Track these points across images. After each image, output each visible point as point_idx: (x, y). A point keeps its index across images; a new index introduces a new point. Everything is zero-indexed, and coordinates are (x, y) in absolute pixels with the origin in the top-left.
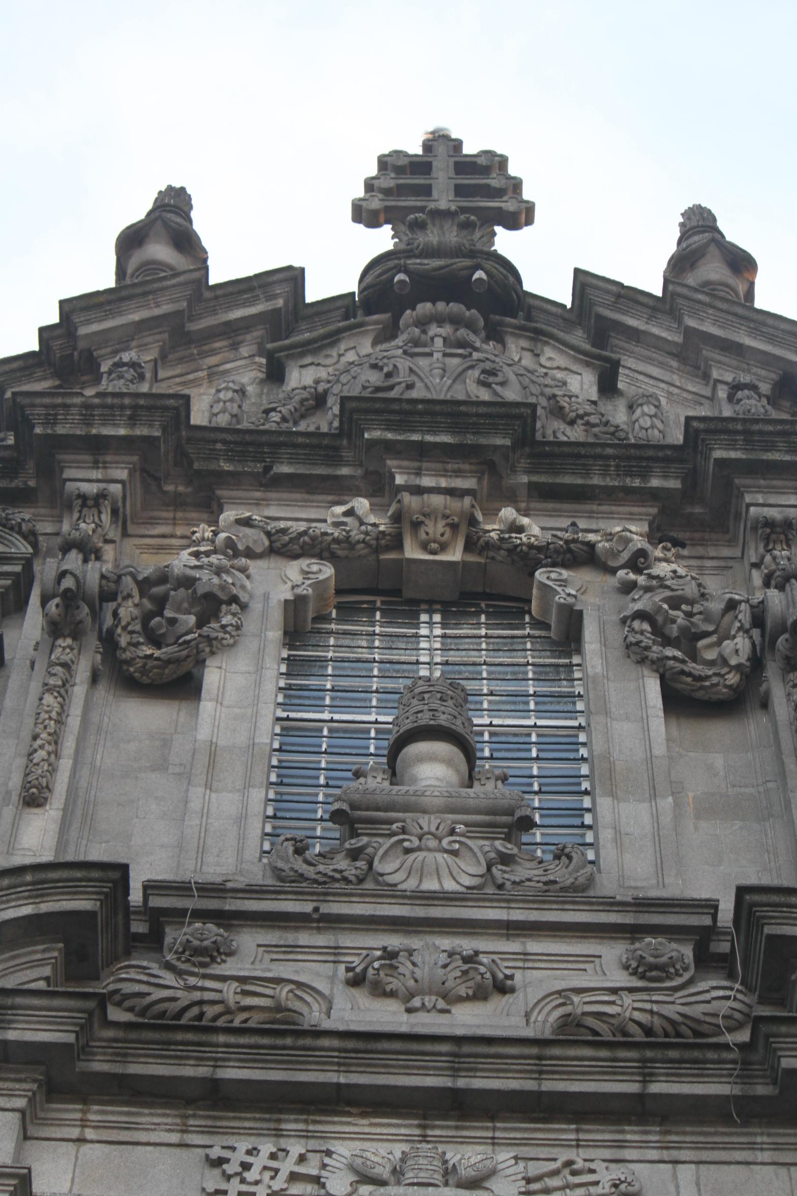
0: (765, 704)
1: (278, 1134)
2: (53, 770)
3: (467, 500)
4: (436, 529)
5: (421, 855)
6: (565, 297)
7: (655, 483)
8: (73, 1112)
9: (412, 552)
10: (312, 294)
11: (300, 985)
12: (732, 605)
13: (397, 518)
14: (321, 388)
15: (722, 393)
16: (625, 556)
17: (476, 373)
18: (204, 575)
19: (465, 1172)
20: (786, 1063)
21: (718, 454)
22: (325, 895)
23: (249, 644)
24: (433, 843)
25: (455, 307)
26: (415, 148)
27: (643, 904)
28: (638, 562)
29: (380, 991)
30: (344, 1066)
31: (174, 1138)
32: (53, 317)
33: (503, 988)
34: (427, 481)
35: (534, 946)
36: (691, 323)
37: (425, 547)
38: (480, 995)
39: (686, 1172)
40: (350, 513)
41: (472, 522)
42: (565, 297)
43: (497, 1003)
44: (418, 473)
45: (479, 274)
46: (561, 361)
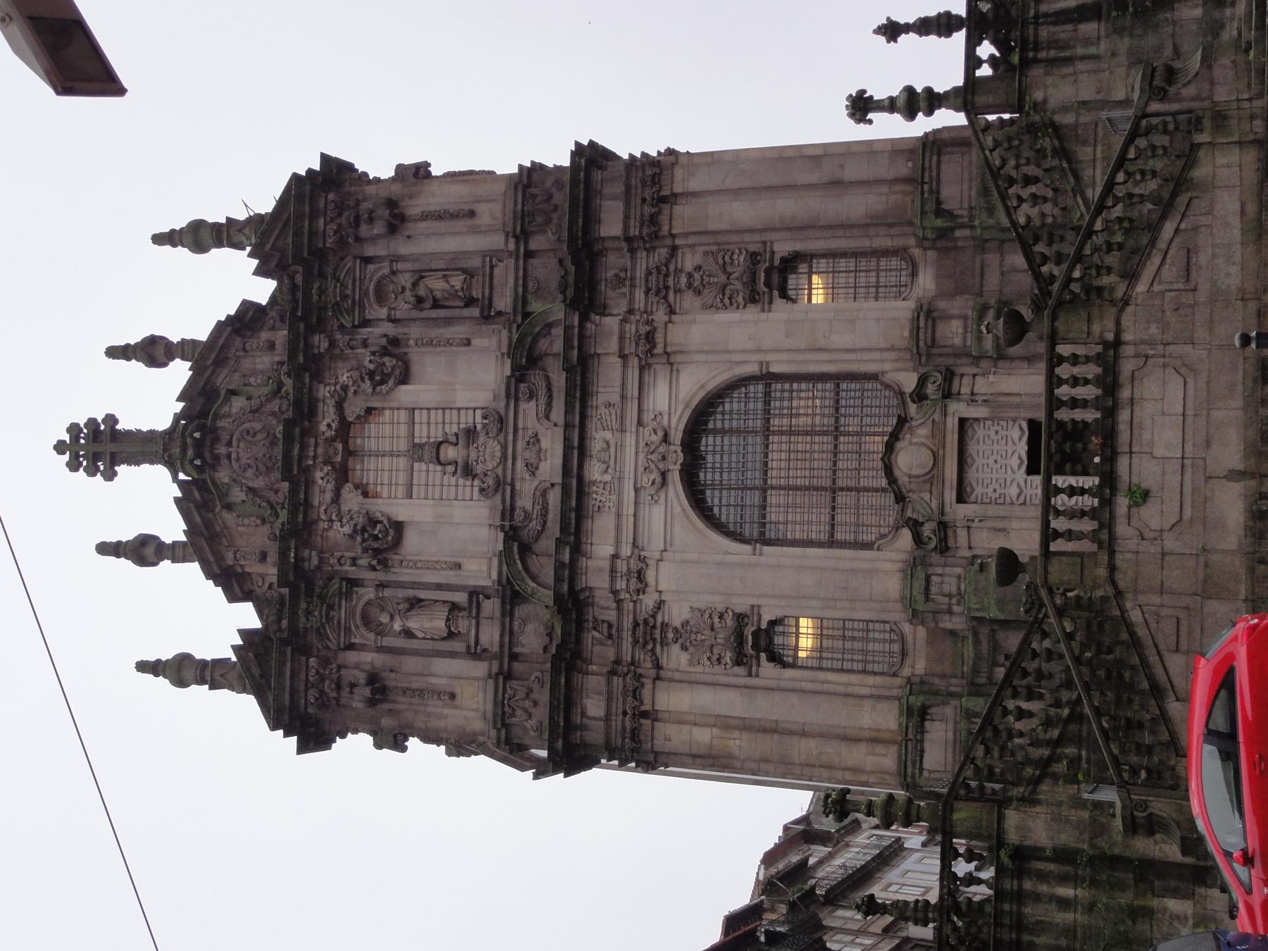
0: (406, 354)
1: (589, 493)
2: (446, 563)
3: (320, 441)
4: (331, 451)
5: (487, 457)
6: (182, 405)
7: (307, 380)
8: (583, 547)
9: (339, 458)
10: (180, 495)
11: (536, 488)
12: (371, 361)
13: (325, 463)
14: (244, 488)
15: (242, 354)
16: (341, 392)
17: (248, 438)
18: (352, 523)
19: (605, 446)
20: (575, 363)
21: (301, 359)
22: (505, 483)
23: (383, 508)
24: (481, 454)
25: (208, 442)
26: (66, 457)
27: (508, 396)
28: (345, 388)
29: (537, 468)
30: (571, 477)
31: (590, 520)
32: (211, 582)
33: (536, 435)
34: (312, 454)
35: (520, 425)
36: (209, 362)
37: (336, 454)
38: (538, 441)
39: (600, 390)
40: (322, 479)
41: (326, 439)
42: (182, 405)
43: (540, 437)
44: (307, 457)
45: (197, 435)
46: (226, 409)
